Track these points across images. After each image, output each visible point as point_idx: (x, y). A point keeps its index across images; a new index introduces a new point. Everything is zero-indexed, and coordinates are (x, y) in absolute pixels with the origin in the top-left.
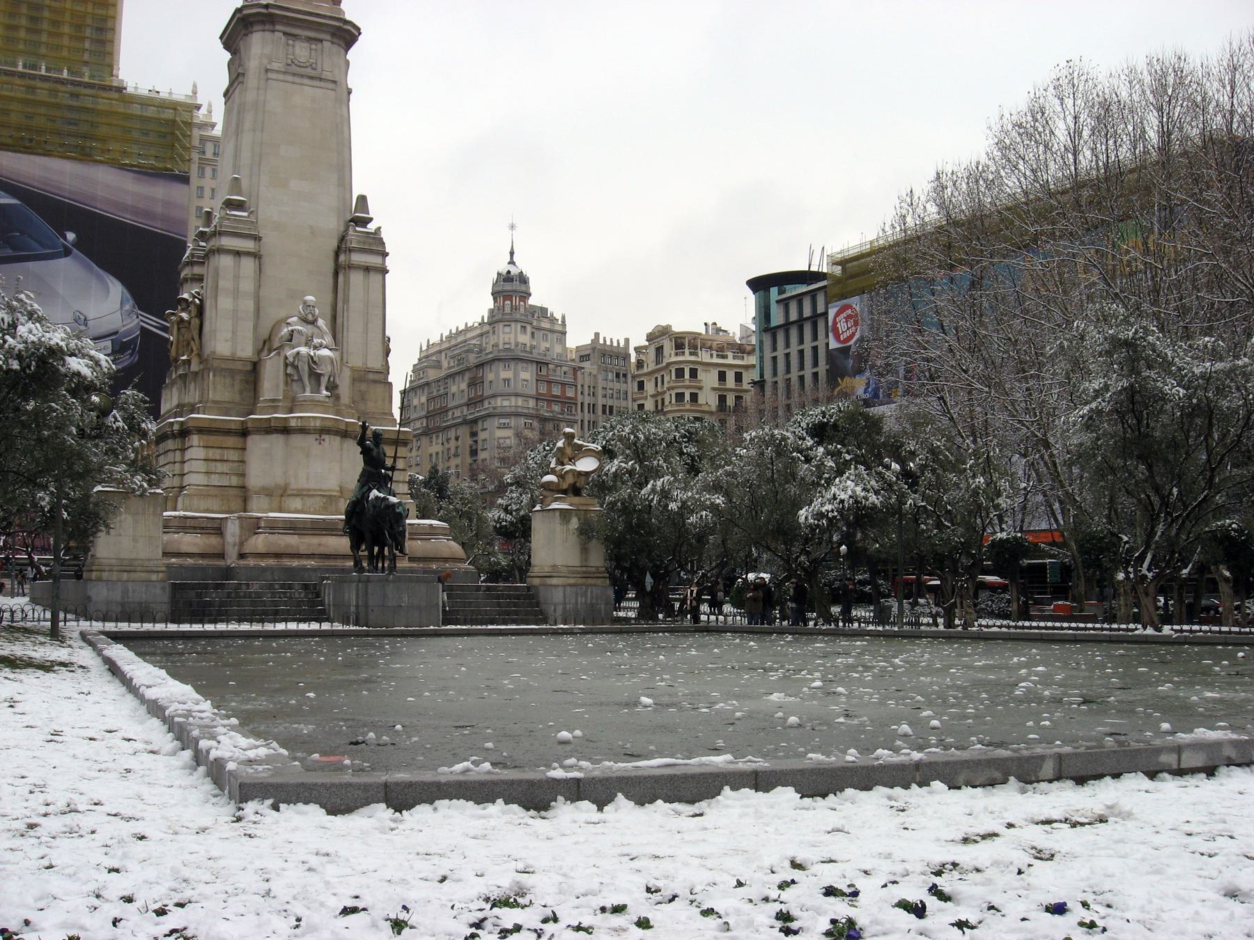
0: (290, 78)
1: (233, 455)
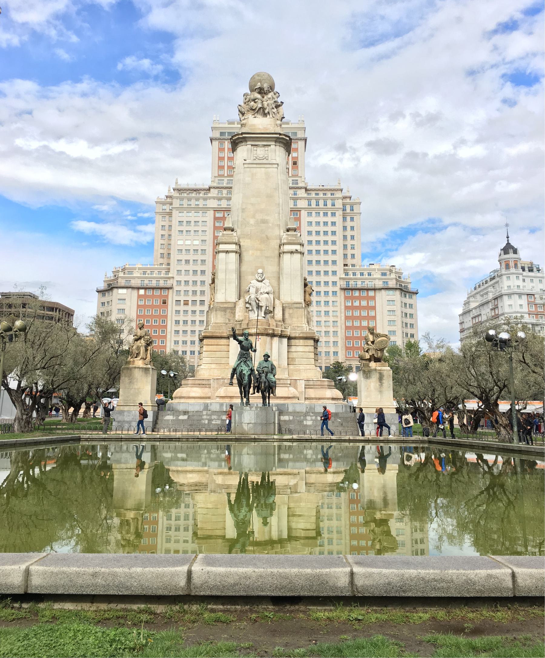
0: (255, 166)
1: (224, 348)
